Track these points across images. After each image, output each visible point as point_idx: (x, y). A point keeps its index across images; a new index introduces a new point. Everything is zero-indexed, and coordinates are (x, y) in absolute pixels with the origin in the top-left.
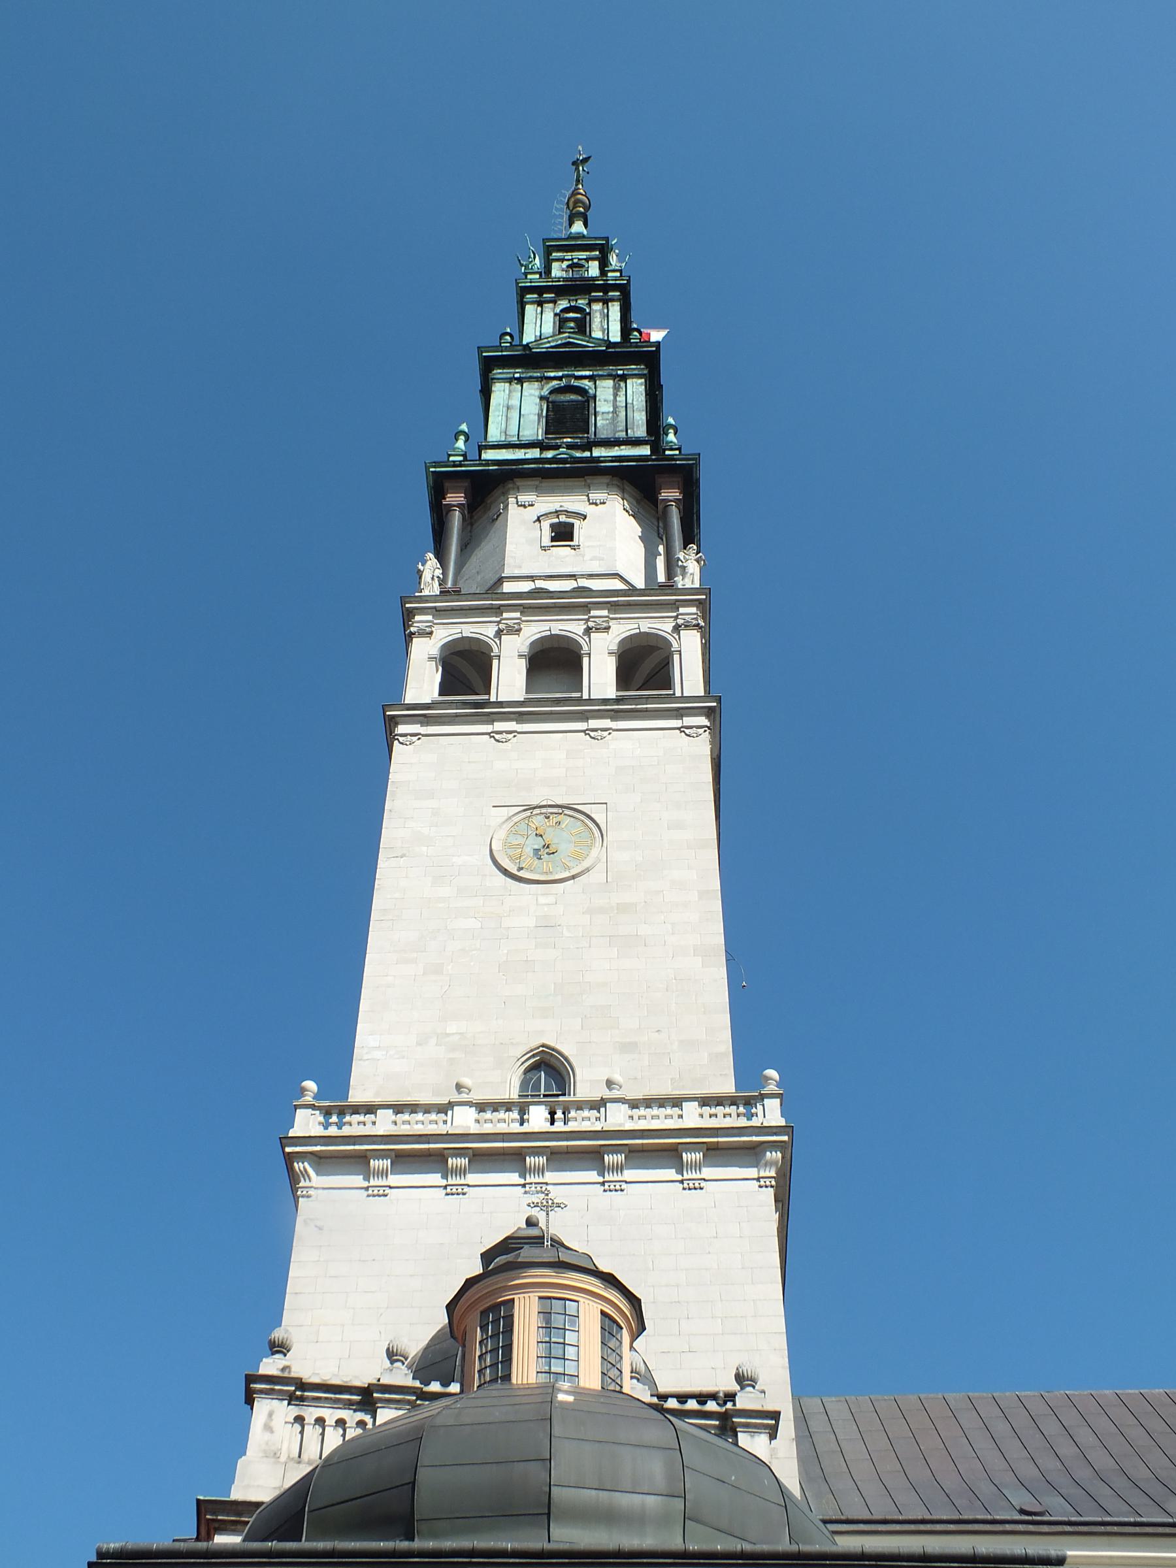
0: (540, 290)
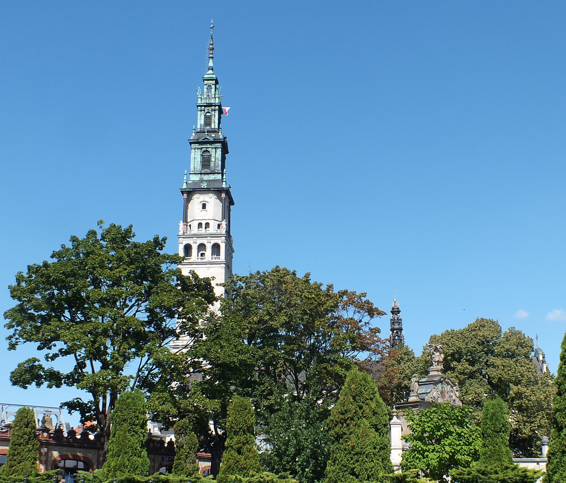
0: (201, 106)
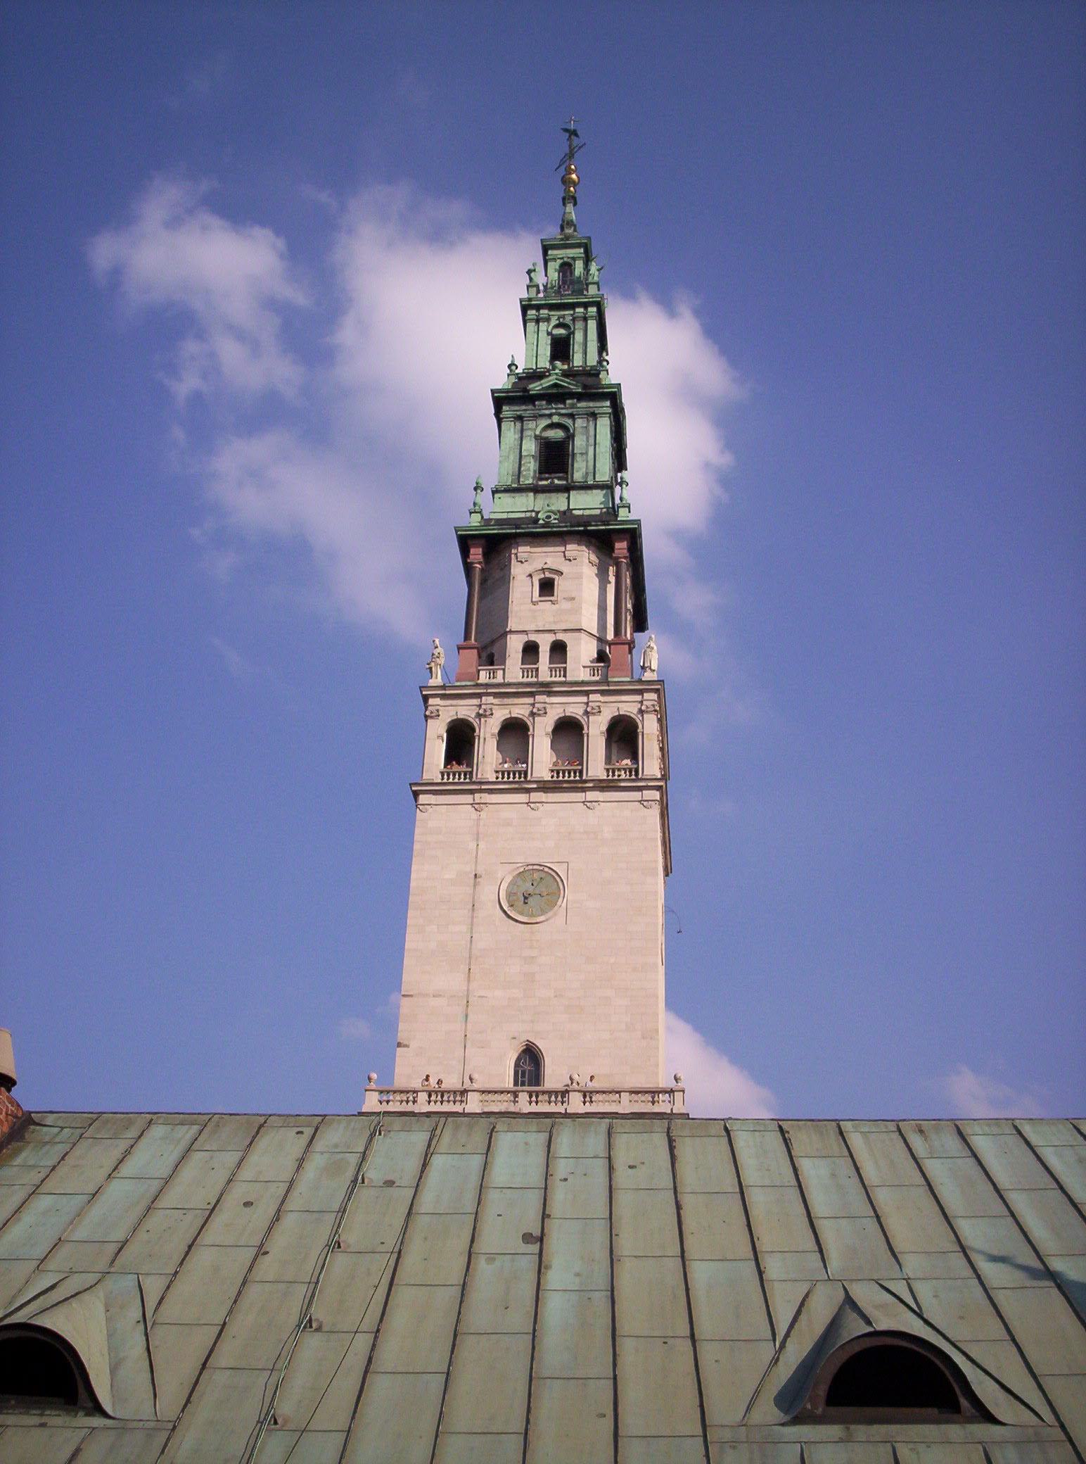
0: (538, 308)
